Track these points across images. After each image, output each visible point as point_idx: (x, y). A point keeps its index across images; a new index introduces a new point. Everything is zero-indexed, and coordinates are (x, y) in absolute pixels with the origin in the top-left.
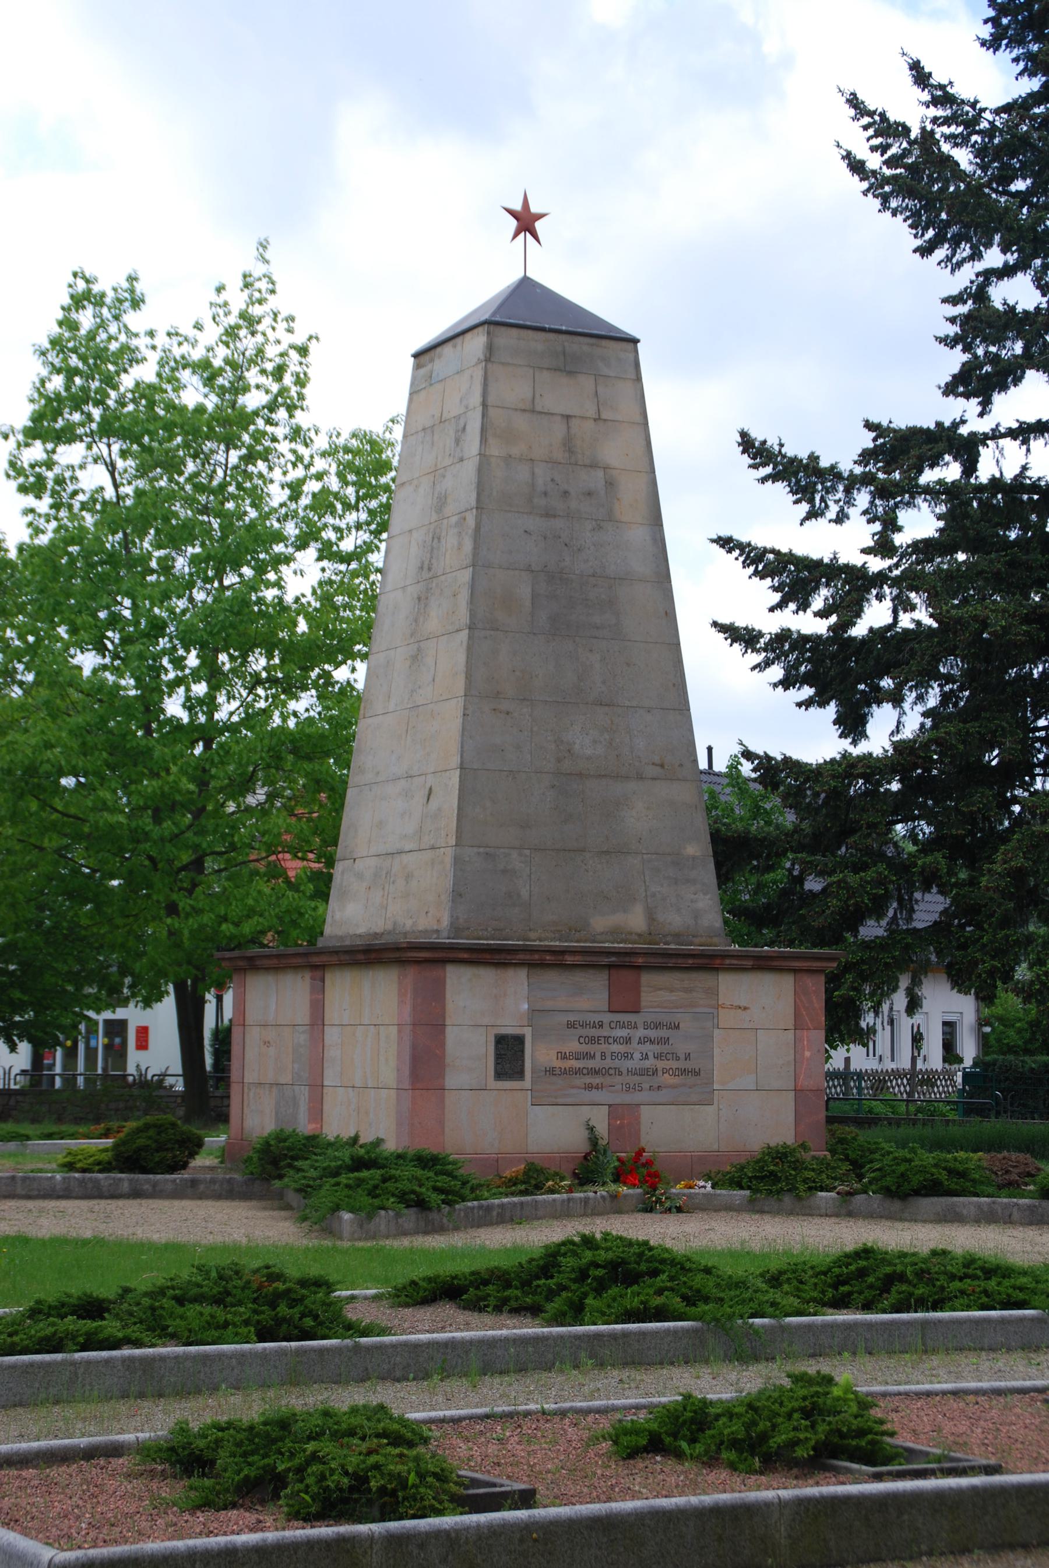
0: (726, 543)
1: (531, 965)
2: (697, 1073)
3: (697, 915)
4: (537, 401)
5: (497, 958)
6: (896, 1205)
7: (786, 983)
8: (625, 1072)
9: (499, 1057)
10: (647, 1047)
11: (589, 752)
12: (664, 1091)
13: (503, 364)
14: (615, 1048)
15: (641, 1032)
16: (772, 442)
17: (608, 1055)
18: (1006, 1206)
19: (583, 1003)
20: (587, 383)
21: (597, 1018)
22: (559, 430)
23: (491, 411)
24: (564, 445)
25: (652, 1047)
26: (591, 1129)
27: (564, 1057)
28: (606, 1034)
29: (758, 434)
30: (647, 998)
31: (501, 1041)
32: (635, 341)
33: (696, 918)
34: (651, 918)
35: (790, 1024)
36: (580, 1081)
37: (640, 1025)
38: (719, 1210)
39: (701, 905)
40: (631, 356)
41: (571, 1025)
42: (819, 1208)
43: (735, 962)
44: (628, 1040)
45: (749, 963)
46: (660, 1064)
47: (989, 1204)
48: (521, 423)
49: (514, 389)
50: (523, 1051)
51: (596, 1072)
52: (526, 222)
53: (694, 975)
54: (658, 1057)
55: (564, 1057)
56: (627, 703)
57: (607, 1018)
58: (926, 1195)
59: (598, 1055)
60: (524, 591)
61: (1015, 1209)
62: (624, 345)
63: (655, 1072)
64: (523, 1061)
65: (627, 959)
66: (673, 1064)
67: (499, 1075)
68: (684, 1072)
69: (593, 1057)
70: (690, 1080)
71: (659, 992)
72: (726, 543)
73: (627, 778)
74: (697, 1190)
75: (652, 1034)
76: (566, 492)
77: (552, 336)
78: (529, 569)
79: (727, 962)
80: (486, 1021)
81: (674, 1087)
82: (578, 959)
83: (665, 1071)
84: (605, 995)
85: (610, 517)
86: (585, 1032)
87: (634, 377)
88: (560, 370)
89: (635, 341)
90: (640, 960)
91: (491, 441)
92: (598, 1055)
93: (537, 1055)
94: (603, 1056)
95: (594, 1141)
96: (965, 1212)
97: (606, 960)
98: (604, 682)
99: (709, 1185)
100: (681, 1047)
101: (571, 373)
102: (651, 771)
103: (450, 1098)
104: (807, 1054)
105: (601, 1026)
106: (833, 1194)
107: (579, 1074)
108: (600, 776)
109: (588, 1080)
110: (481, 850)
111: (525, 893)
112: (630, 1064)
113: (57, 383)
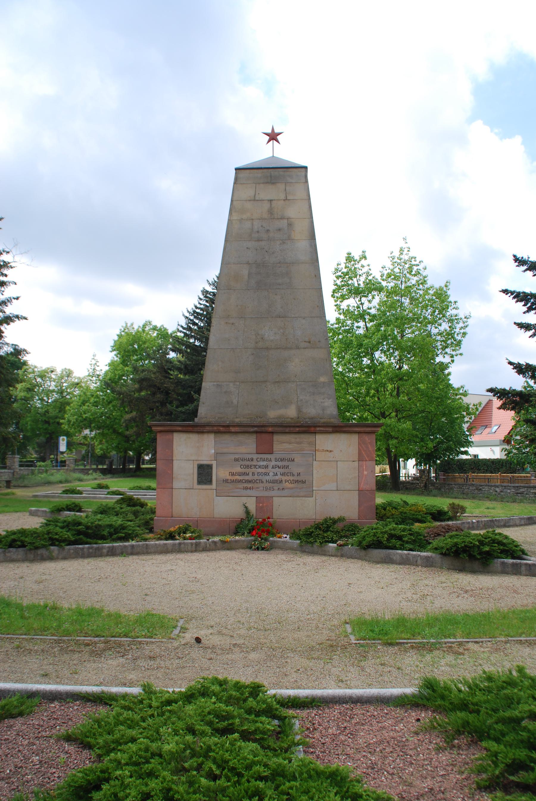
0: (505, 292)
1: (217, 432)
2: (304, 482)
3: (324, 409)
4: (256, 196)
6: (363, 553)
7: (355, 438)
8: (265, 482)
9: (199, 474)
11: (272, 338)
12: (286, 490)
14: (260, 470)
15: (273, 463)
16: (525, 257)
18: (415, 556)
19: (242, 449)
20: (282, 186)
21: (250, 456)
22: (266, 206)
23: (234, 203)
24: (269, 211)
25: (279, 470)
26: (246, 507)
27: (233, 474)
28: (255, 464)
29: (519, 256)
30: (276, 447)
31: (201, 467)
32: (306, 168)
33: (323, 410)
34: (299, 410)
35: (356, 458)
36: (241, 485)
37: (273, 460)
38: (287, 550)
40: (303, 174)
41: (236, 460)
42: (329, 552)
43: (322, 429)
44: (267, 467)
45: (330, 429)
46: (284, 478)
47: (406, 555)
48: (249, 205)
49: (248, 192)
51: (250, 482)
52: (273, 137)
53: (302, 436)
54: (283, 474)
55: (233, 474)
56: (293, 316)
57: (255, 456)
58: (376, 548)
59: (251, 474)
60: (245, 272)
61: (419, 558)
62: (300, 169)
63: (281, 481)
64: (212, 476)
65: (263, 429)
66: (291, 478)
67: (200, 482)
68: (297, 481)
69: (248, 474)
70: (300, 485)
71: (283, 444)
72: (505, 292)
73: (291, 348)
74: (282, 540)
75: (279, 464)
76: (268, 231)
77: (265, 170)
78: (248, 263)
79: (318, 429)
80: (193, 458)
81: (292, 488)
82: (237, 429)
84: (255, 446)
85: (289, 238)
86: (242, 463)
87: (304, 181)
89: (306, 168)
90: (270, 429)
91: (233, 214)
92: (251, 474)
94: (253, 474)
95: (247, 512)
96: (394, 558)
97: (252, 430)
98: (282, 308)
99: (288, 537)
100: (295, 470)
101: (273, 183)
104: (365, 473)
105: (252, 460)
106: (335, 545)
107: (239, 483)
109: (246, 485)
110: (215, 383)
111: (235, 402)
112: (267, 478)
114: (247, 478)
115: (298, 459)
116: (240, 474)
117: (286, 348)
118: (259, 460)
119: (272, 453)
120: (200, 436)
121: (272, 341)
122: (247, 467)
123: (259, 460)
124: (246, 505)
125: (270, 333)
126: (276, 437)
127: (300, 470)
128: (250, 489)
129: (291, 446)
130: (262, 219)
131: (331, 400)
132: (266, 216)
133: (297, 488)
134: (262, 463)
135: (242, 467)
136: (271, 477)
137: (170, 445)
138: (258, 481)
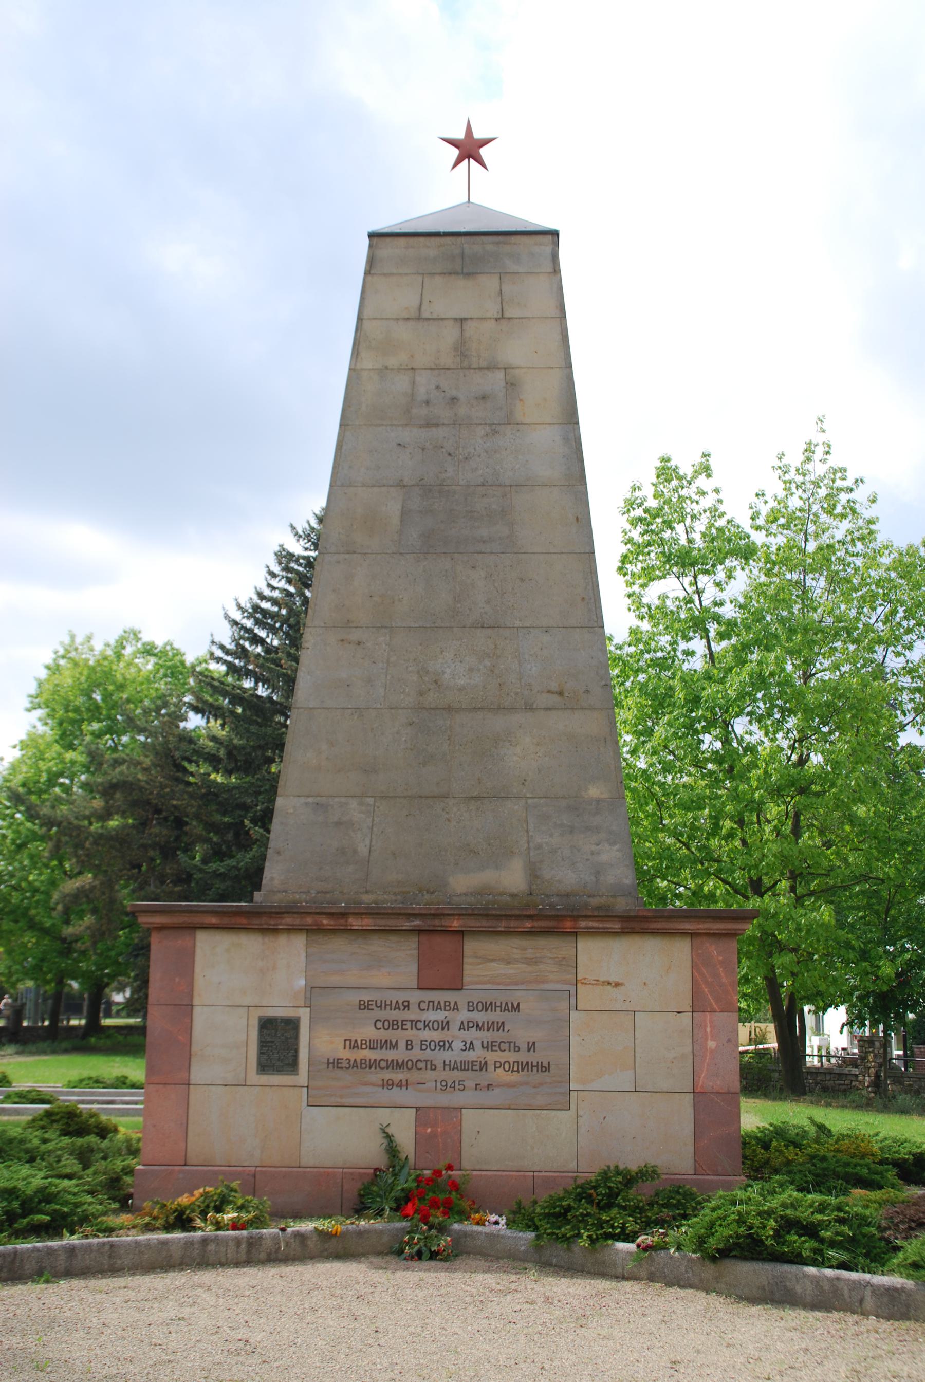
1: (314, 931)
2: (545, 1068)
4: (424, 308)
5: (264, 921)
6: (710, 1270)
7: (681, 949)
8: (440, 1066)
9: (264, 1045)
10: (473, 1035)
11: (462, 682)
12: (497, 1091)
13: (385, 275)
14: (427, 1035)
15: (464, 1015)
17: (416, 1044)
18: (856, 1286)
19: (381, 978)
20: (490, 283)
21: (401, 997)
22: (450, 334)
23: (366, 324)
24: (456, 349)
26: (389, 1137)
27: (354, 1045)
28: (413, 1017)
30: (471, 972)
31: (267, 1024)
32: (555, 234)
33: (597, 873)
34: (533, 873)
35: (686, 1005)
37: (463, 1006)
38: (498, 1258)
39: (604, 858)
40: (548, 249)
41: (364, 1006)
42: (615, 1265)
43: (595, 924)
44: (445, 1025)
45: (617, 926)
46: (491, 1057)
47: (830, 1280)
48: (403, 332)
49: (401, 297)
50: (296, 1037)
51: (399, 1065)
52: (469, 149)
53: (542, 942)
54: (489, 1046)
56: (518, 623)
57: (415, 997)
58: (745, 1259)
59: (402, 1045)
60: (392, 508)
61: (868, 1292)
62: (539, 238)
63: (484, 1066)
64: (297, 1051)
65: (437, 922)
66: (512, 1057)
67: (264, 1067)
68: (526, 1066)
70: (536, 1077)
71: (489, 964)
73: (512, 709)
75: (480, 1017)
76: (454, 400)
77: (448, 240)
78: (400, 484)
79: (583, 924)
80: (248, 1001)
83: (497, 1065)
84: (414, 968)
85: (509, 420)
87: (551, 270)
88: (458, 274)
89: (555, 234)
90: (456, 924)
91: (363, 354)
92: (402, 1045)
93: (316, 1042)
94: (409, 1045)
95: (392, 1150)
96: (798, 1289)
97: (407, 925)
98: (488, 602)
99: (503, 1221)
101: (468, 275)
102: (544, 700)
103: (196, 1095)
104: (711, 1044)
105: (407, 1006)
106: (632, 1247)
108: (476, 709)
109: (388, 1075)
110: (310, 800)
111: (363, 849)
112: (447, 1055)
113: (635, 534)
114: (391, 1055)
115: (530, 1004)
116: (374, 1045)
117: (499, 709)
118: (424, 1006)
119: (458, 987)
120: (269, 940)
121: (461, 689)
122: (394, 1025)
123: (424, 1006)
124: (390, 1131)
125: (457, 668)
126: (471, 946)
127: (536, 1034)
128: (400, 1085)
129: (510, 970)
130: (438, 369)
131: (615, 848)
132: (447, 360)
133: (526, 1084)
134: (432, 1016)
135: (379, 1025)
136: (455, 1054)
137: (185, 966)
138: (420, 1065)
